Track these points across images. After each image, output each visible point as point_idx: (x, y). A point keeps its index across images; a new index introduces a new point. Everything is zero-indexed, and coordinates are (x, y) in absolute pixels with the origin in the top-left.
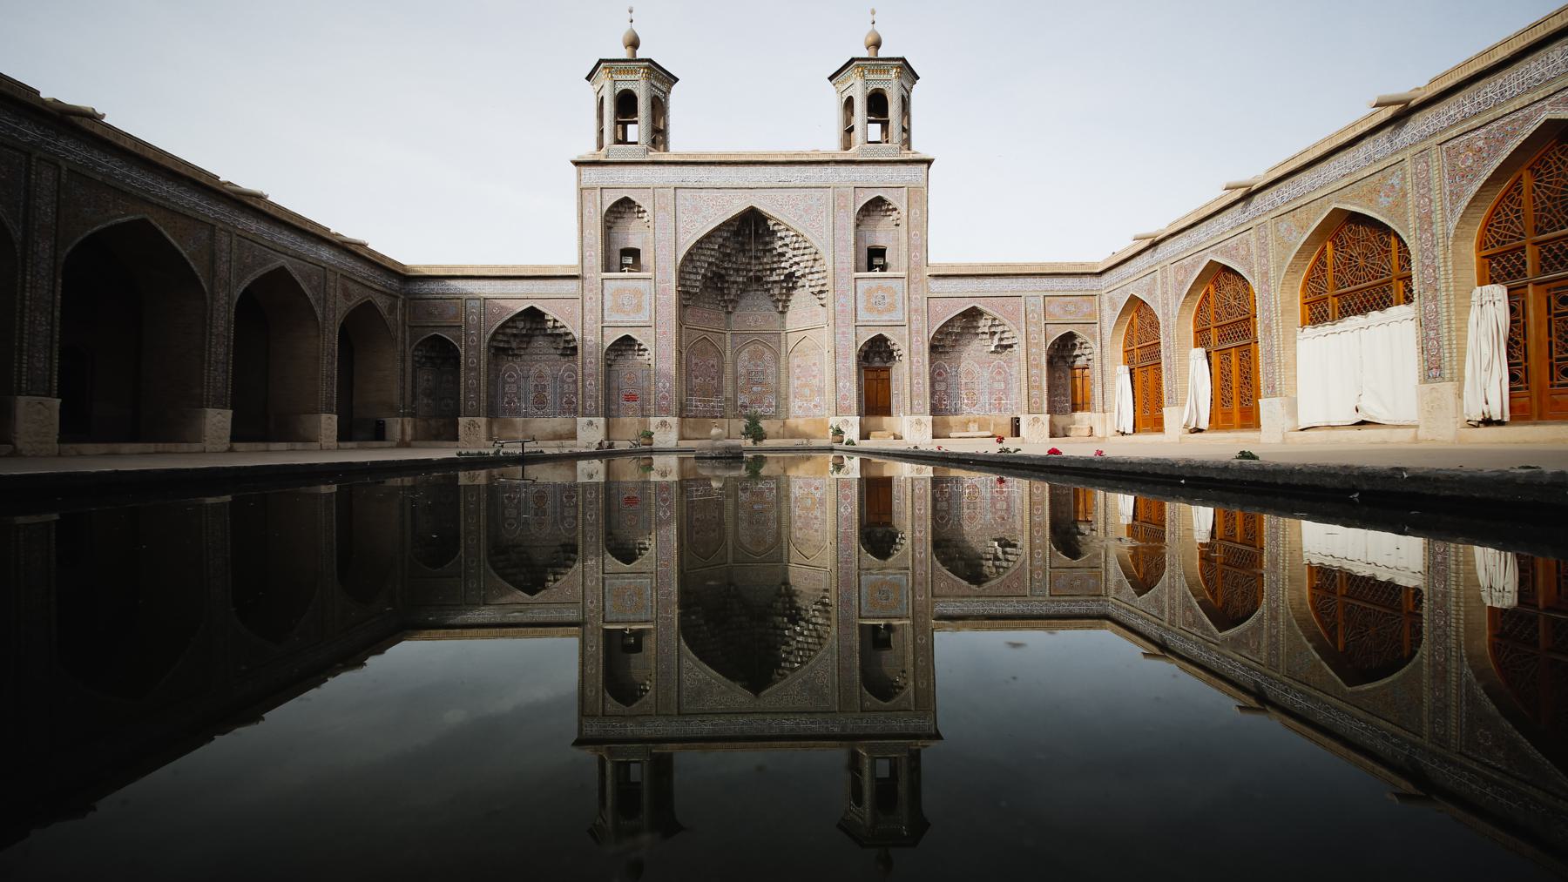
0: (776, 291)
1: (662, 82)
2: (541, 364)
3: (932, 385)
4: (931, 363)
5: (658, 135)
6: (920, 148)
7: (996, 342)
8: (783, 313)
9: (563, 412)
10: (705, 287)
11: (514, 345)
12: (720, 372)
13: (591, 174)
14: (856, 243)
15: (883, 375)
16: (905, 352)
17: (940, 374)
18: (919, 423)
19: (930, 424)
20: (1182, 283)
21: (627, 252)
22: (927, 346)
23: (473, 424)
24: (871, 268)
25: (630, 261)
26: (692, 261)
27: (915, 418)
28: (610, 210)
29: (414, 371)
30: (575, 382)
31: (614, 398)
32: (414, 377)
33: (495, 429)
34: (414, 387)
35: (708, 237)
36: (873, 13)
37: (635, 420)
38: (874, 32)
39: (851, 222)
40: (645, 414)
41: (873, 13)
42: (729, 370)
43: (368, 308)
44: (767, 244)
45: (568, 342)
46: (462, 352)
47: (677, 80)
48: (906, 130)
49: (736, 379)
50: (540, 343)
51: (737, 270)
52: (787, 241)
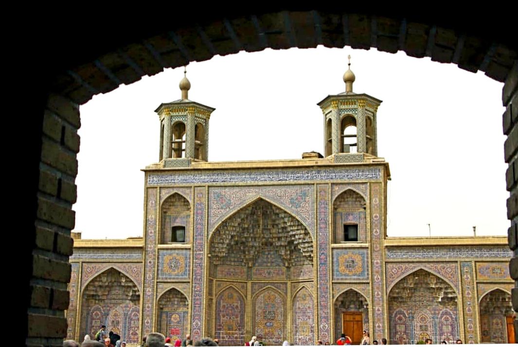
1: (203, 113)
7: (442, 295)
8: (288, 268)
11: (100, 293)
13: (155, 180)
14: (334, 222)
15: (358, 318)
16: (369, 302)
17: (400, 319)
28: (165, 201)
35: (230, 218)
36: (349, 57)
39: (330, 207)
42: (249, 309)
44: (274, 221)
45: (135, 291)
47: (214, 109)
49: (254, 318)
50: (117, 292)
52: (286, 220)
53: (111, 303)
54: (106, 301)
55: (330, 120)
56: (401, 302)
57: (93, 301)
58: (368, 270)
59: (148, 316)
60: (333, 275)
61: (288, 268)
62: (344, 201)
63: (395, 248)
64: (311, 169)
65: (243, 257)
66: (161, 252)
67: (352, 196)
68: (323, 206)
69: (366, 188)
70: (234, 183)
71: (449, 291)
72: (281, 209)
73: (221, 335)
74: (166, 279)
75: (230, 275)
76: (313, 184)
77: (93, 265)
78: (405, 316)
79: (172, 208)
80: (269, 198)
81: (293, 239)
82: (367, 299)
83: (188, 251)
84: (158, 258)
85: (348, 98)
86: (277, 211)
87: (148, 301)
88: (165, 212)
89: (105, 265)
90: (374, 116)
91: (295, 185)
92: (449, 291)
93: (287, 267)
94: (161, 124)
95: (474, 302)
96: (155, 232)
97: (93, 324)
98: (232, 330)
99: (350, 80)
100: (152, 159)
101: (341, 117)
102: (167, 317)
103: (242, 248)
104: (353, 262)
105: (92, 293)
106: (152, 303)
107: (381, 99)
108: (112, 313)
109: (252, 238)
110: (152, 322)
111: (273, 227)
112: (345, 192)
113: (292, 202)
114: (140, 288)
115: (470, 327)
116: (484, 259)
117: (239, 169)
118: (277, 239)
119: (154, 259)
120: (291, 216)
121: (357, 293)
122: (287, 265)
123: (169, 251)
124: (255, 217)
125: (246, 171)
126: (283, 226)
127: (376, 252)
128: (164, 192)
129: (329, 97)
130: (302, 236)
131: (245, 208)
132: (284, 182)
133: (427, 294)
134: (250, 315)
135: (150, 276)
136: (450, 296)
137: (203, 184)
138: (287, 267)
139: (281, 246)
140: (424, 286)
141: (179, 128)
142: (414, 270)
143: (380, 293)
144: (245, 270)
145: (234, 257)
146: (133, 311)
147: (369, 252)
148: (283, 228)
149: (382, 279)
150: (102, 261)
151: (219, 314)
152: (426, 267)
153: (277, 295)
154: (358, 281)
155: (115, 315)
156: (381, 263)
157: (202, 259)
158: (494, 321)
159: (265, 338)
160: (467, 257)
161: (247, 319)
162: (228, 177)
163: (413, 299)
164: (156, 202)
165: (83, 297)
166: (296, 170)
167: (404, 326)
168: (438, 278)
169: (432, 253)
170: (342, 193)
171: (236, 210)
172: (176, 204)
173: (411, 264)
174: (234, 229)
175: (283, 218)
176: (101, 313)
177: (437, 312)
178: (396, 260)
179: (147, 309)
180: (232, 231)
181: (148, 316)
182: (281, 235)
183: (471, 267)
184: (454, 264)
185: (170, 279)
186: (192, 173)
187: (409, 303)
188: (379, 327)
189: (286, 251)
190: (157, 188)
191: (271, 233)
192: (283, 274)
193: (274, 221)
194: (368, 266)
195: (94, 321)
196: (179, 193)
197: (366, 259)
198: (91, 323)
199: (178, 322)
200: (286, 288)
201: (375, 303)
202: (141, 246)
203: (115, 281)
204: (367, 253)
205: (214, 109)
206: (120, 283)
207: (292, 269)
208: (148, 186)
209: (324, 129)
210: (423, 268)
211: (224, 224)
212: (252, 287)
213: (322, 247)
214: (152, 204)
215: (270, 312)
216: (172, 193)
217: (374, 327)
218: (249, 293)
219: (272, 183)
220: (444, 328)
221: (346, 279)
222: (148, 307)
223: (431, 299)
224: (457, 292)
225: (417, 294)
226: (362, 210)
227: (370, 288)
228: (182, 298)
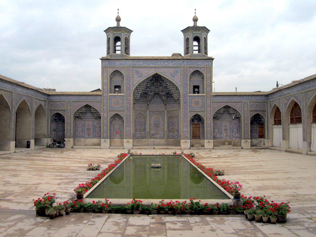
0: (164, 98)
1: (128, 33)
2: (89, 122)
3: (214, 129)
4: (213, 123)
5: (127, 49)
6: (210, 55)
9: (96, 137)
10: (141, 97)
11: (81, 116)
12: (145, 124)
13: (106, 63)
15: (198, 126)
16: (205, 120)
18: (209, 142)
19: (212, 142)
20: (286, 104)
21: (116, 87)
22: (212, 117)
23: (69, 141)
24: (194, 92)
25: (117, 89)
26: (137, 89)
27: (208, 141)
28: (112, 74)
29: (51, 123)
30: (100, 127)
31: (112, 133)
32: (51, 125)
33: (76, 142)
34: (51, 129)
35: (142, 82)
37: (119, 140)
38: (195, 16)
39: (189, 78)
40: (122, 138)
41: (195, 10)
43: (41, 106)
45: (98, 115)
46: (66, 118)
47: (132, 31)
48: (206, 48)
49: (150, 126)
51: (151, 91)
52: (167, 83)
53: (86, 120)
54: (84, 119)
56: (217, 119)
57: (78, 119)
58: (205, 106)
59: (105, 126)
60: (189, 108)
62: (194, 75)
63: (217, 96)
64: (180, 60)
65: (145, 100)
66: (111, 97)
67: (197, 73)
68: (185, 77)
69: (204, 70)
70: (144, 66)
71: (237, 114)
72: (166, 78)
73: (137, 134)
74: (113, 109)
75: (140, 107)
76: (181, 67)
77: (78, 103)
78: (218, 125)
79: (114, 77)
80: (161, 73)
81: (169, 92)
82: (204, 118)
83: (123, 96)
84: (109, 100)
85: (195, 28)
86: (164, 79)
87: (105, 119)
88: (111, 79)
89: (83, 103)
90: (207, 37)
91: (173, 67)
92: (237, 114)
93: (165, 104)
94: (107, 37)
95: (248, 119)
96: (107, 88)
97: (78, 129)
98: (141, 131)
99: (195, 20)
100: (104, 54)
101: (194, 37)
102: (113, 126)
103: (145, 96)
104: (198, 102)
105: (77, 116)
106: (107, 120)
107: (210, 30)
108: (87, 124)
109: (150, 91)
110: (107, 129)
111: (160, 86)
112: (194, 71)
113: (171, 75)
115: (246, 129)
116: (253, 101)
117: (147, 59)
118: (161, 92)
119: (107, 100)
120: (170, 81)
121: (199, 115)
122: (165, 103)
123: (114, 97)
124: (152, 82)
125: (150, 60)
126: (165, 86)
127: (208, 98)
128: (111, 69)
129: (189, 27)
130: (174, 91)
132: (167, 66)
133: (228, 115)
134: (148, 125)
135: (105, 108)
136: (238, 116)
137: (130, 66)
138: (165, 104)
139: (163, 95)
140: (227, 112)
142: (224, 106)
143: (210, 115)
144: (146, 105)
145: (142, 100)
146: (97, 124)
147: (205, 98)
148: (165, 87)
149: (211, 109)
150: (82, 101)
151: (136, 125)
152: (229, 104)
153: (160, 117)
154: (200, 110)
155: (89, 126)
156: (211, 102)
157: (130, 100)
158: (254, 126)
159: (155, 135)
160: (246, 100)
163: (222, 118)
164: (107, 74)
165: (74, 118)
166: (173, 61)
167: (218, 129)
168: (234, 109)
169: (232, 98)
170: (193, 72)
171: (145, 79)
172: (116, 75)
173: (223, 103)
174: (144, 87)
176: (82, 125)
177: (231, 123)
178: (216, 101)
179: (105, 123)
180: (143, 88)
181: (105, 126)
182: (163, 90)
183: (247, 104)
184: (240, 103)
185: (115, 109)
186: (124, 60)
187: (220, 120)
188: (209, 129)
189: (165, 97)
190: (107, 67)
191: (159, 89)
192: (163, 107)
193: (161, 83)
194: (204, 104)
195: (79, 128)
196: (119, 70)
197: (204, 101)
198: (77, 129)
199: (119, 129)
200: (165, 114)
201: (208, 120)
202: (101, 94)
203: (88, 110)
204: (205, 98)
205: (132, 31)
206: (91, 111)
207: (167, 105)
208: (103, 66)
209: (184, 43)
210: (228, 105)
211: (140, 85)
212: (149, 114)
213: (185, 96)
214: (105, 75)
215: (157, 124)
216: (115, 70)
217: (207, 129)
218: (148, 116)
219: (162, 66)
220: (234, 129)
221: (195, 110)
222: (105, 122)
223: (229, 118)
224: (241, 114)
225: (224, 115)
226: (202, 79)
227: (206, 113)
228: (120, 118)
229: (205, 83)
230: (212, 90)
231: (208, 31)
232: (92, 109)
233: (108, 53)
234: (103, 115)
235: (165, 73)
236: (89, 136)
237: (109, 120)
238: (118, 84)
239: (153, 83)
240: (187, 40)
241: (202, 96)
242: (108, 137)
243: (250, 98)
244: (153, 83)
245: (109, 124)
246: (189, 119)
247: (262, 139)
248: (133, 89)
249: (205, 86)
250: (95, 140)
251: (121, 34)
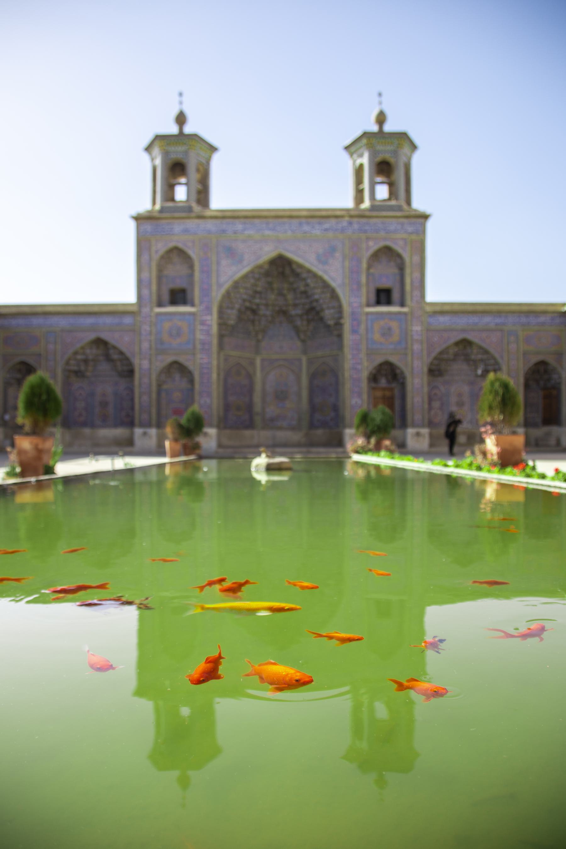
4: (429, 384)
5: (202, 194)
10: (240, 319)
12: (251, 390)
17: (435, 394)
28: (162, 257)
30: (132, 400)
39: (364, 265)
42: (258, 387)
52: (309, 281)
55: (361, 166)
61: (303, 341)
104: (390, 329)
114: (136, 362)
117: (254, 217)
120: (315, 276)
131: (260, 267)
141: (176, 169)
161: (257, 398)
162: (239, 226)
166: (323, 220)
168: (481, 348)
175: (304, 279)
182: (297, 302)
211: (236, 285)
229: (408, 280)
230: (423, 296)
231: (414, 147)
232: (111, 351)
233: (154, 203)
234: (141, 364)
235: (306, 256)
236: (105, 422)
237: (154, 377)
238: (179, 284)
239: (270, 283)
240: (359, 171)
241: (400, 313)
242: (154, 421)
243: (524, 320)
244: (270, 283)
245: (154, 388)
246: (365, 374)
247: (554, 429)
248: (217, 295)
249: (408, 287)
250: (119, 432)
251: (186, 153)
